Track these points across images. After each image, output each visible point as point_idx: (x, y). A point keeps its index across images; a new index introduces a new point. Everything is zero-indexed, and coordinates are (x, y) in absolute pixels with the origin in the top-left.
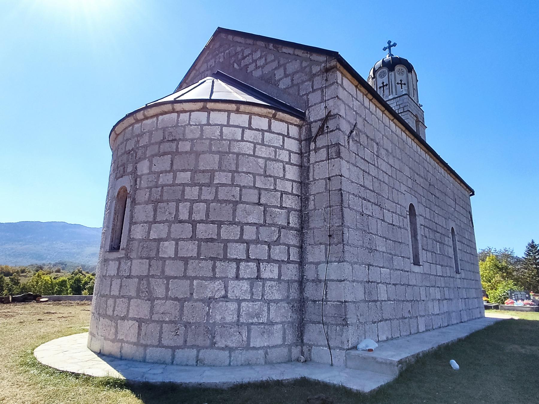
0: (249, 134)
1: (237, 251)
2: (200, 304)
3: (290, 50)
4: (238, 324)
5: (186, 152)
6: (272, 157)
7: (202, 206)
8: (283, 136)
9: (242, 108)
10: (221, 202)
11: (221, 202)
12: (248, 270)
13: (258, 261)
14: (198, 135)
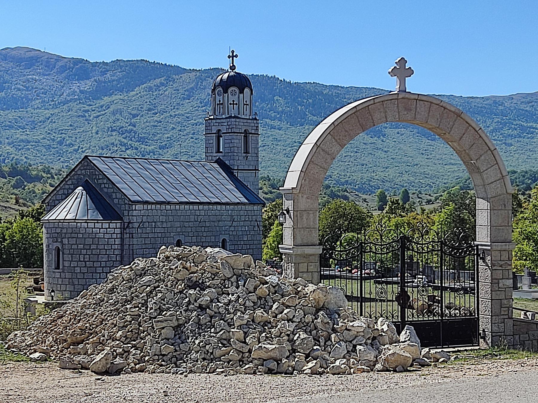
1: (99, 270)
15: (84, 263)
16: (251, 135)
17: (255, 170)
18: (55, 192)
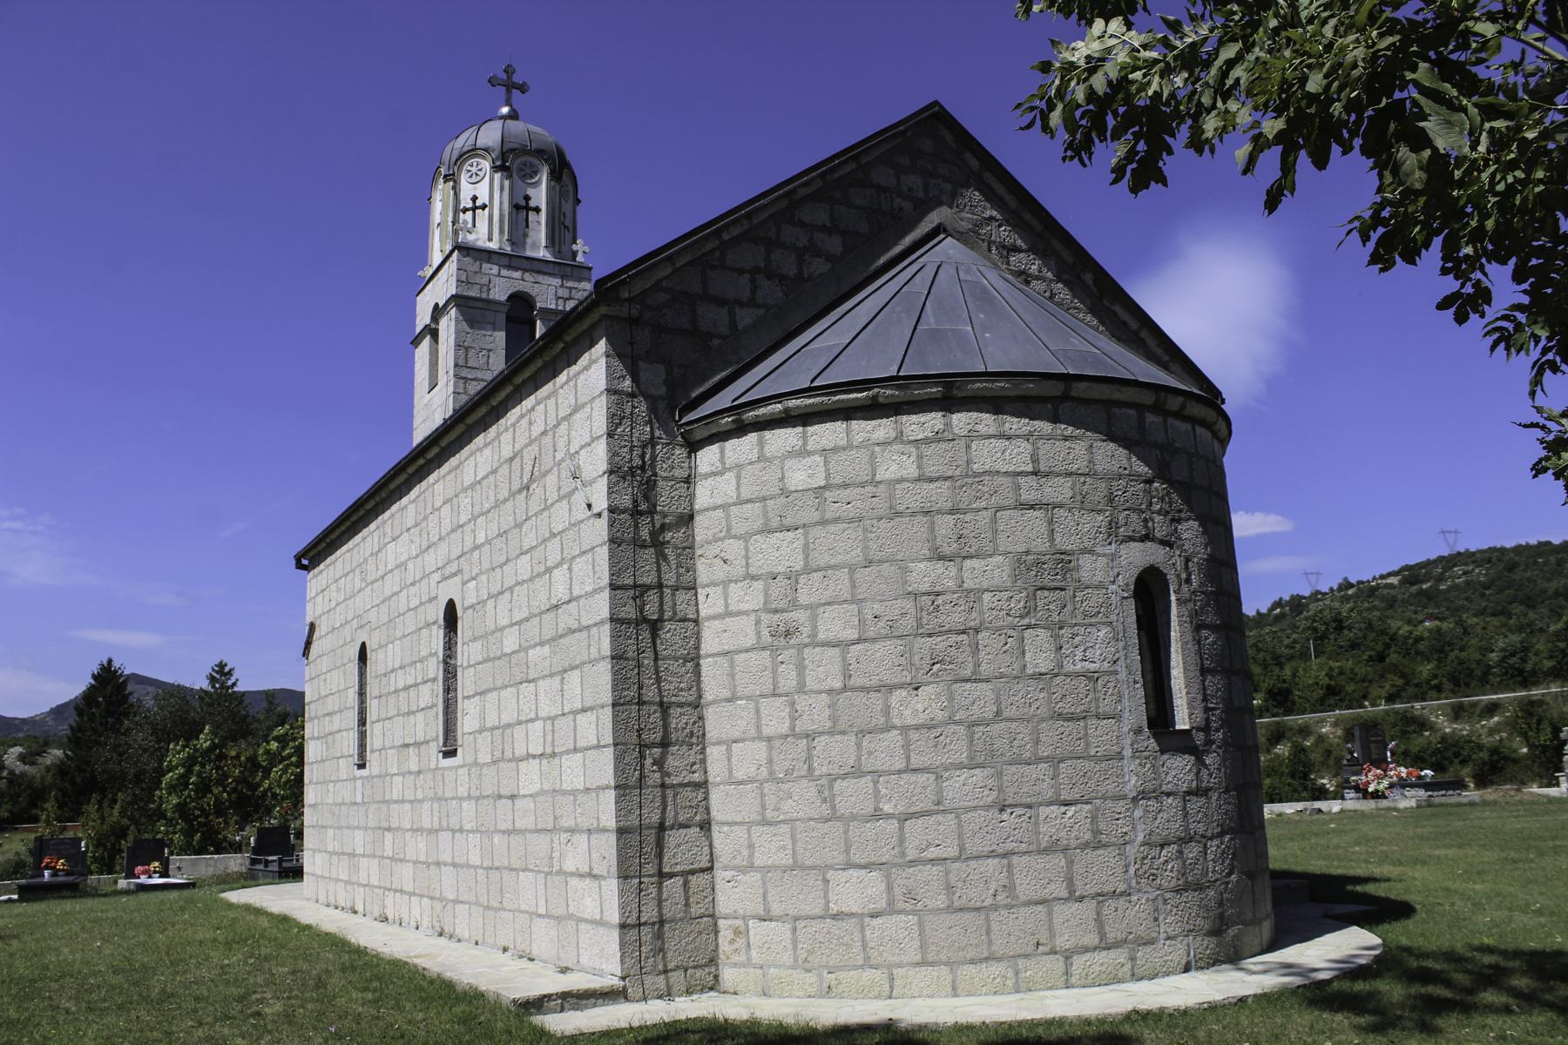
3: (1134, 325)
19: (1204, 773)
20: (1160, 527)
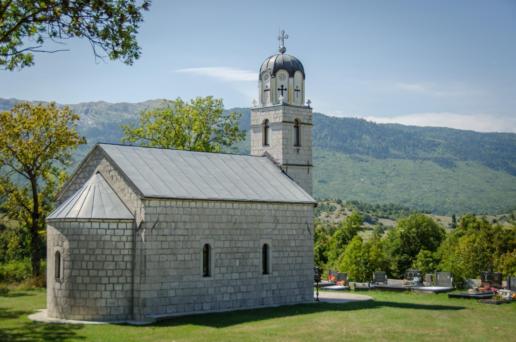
0: (109, 232)
1: (105, 280)
2: (92, 300)
4: (106, 307)
5: (83, 241)
6: (119, 240)
7: (90, 264)
8: (124, 229)
9: (105, 221)
10: (98, 261)
11: (98, 261)
12: (110, 287)
13: (113, 284)
14: (87, 233)
15: (86, 272)
16: (302, 125)
17: (308, 165)
18: (67, 187)
19: (62, 286)
20: (60, 244)
